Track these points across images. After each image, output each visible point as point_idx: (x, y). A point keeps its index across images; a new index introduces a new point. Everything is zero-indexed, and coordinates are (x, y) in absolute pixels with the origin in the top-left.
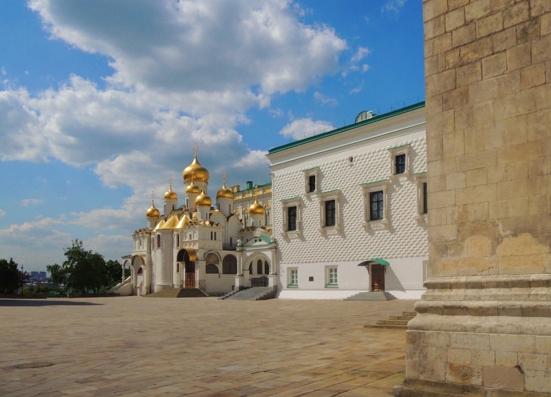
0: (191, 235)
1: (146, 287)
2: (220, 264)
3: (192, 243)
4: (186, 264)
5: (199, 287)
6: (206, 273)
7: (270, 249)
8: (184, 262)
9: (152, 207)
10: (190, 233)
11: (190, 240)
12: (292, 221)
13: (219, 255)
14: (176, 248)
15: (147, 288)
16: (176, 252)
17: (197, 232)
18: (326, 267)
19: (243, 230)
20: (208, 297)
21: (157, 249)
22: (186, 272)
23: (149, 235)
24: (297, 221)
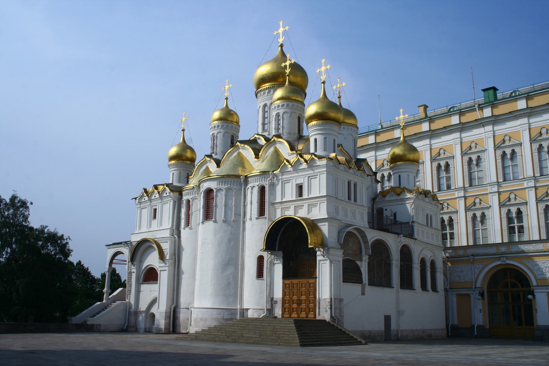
0: (300, 188)
1: (166, 312)
2: (363, 262)
3: (306, 206)
4: (283, 257)
5: (331, 316)
6: (343, 282)
9: (181, 140)
10: (300, 181)
11: (301, 198)
13: (364, 236)
14: (257, 218)
15: (167, 317)
17: (324, 177)
19: (384, 193)
20: (366, 344)
21: (203, 223)
22: (285, 277)
23: (177, 194)
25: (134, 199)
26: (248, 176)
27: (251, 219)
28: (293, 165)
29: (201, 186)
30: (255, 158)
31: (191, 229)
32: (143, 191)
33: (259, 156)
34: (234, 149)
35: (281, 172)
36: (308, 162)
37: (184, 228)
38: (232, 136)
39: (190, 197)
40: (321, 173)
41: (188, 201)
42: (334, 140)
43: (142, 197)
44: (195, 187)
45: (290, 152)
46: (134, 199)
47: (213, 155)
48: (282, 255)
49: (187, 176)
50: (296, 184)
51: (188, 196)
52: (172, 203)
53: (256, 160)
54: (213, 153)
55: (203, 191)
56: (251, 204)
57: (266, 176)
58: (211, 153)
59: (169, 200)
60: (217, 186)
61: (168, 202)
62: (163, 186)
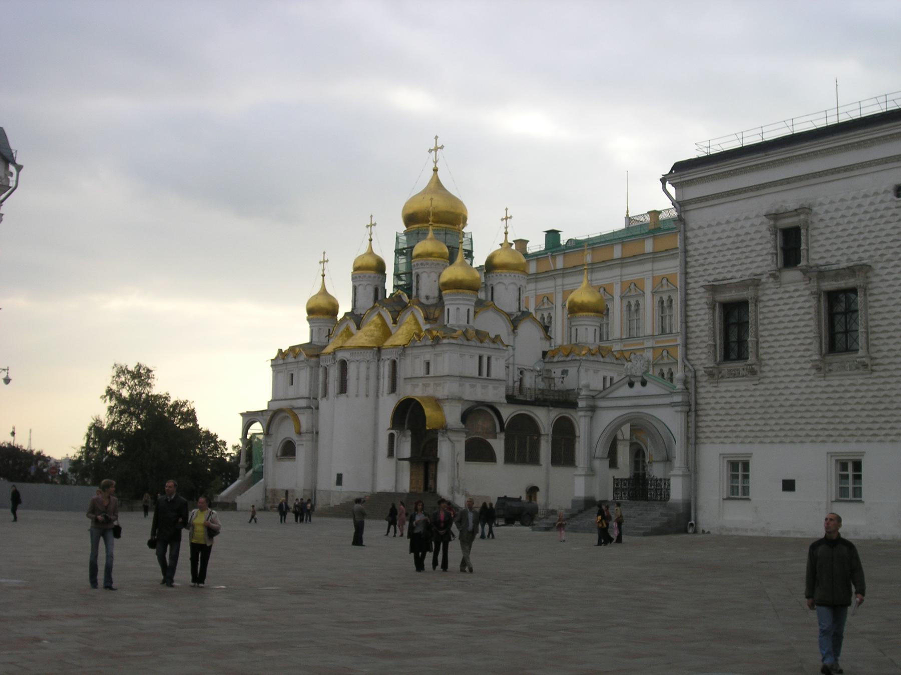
0: (428, 364)
4: (412, 436)
7: (673, 405)
8: (409, 433)
10: (427, 357)
12: (733, 338)
16: (389, 404)
18: (831, 454)
24: (750, 339)
27: (382, 395)
30: (393, 323)
31: (327, 399)
37: (321, 399)
38: (376, 290)
42: (469, 310)
43: (277, 358)
45: (424, 321)
48: (410, 433)
49: (327, 334)
50: (424, 361)
52: (308, 369)
53: (394, 325)
56: (383, 378)
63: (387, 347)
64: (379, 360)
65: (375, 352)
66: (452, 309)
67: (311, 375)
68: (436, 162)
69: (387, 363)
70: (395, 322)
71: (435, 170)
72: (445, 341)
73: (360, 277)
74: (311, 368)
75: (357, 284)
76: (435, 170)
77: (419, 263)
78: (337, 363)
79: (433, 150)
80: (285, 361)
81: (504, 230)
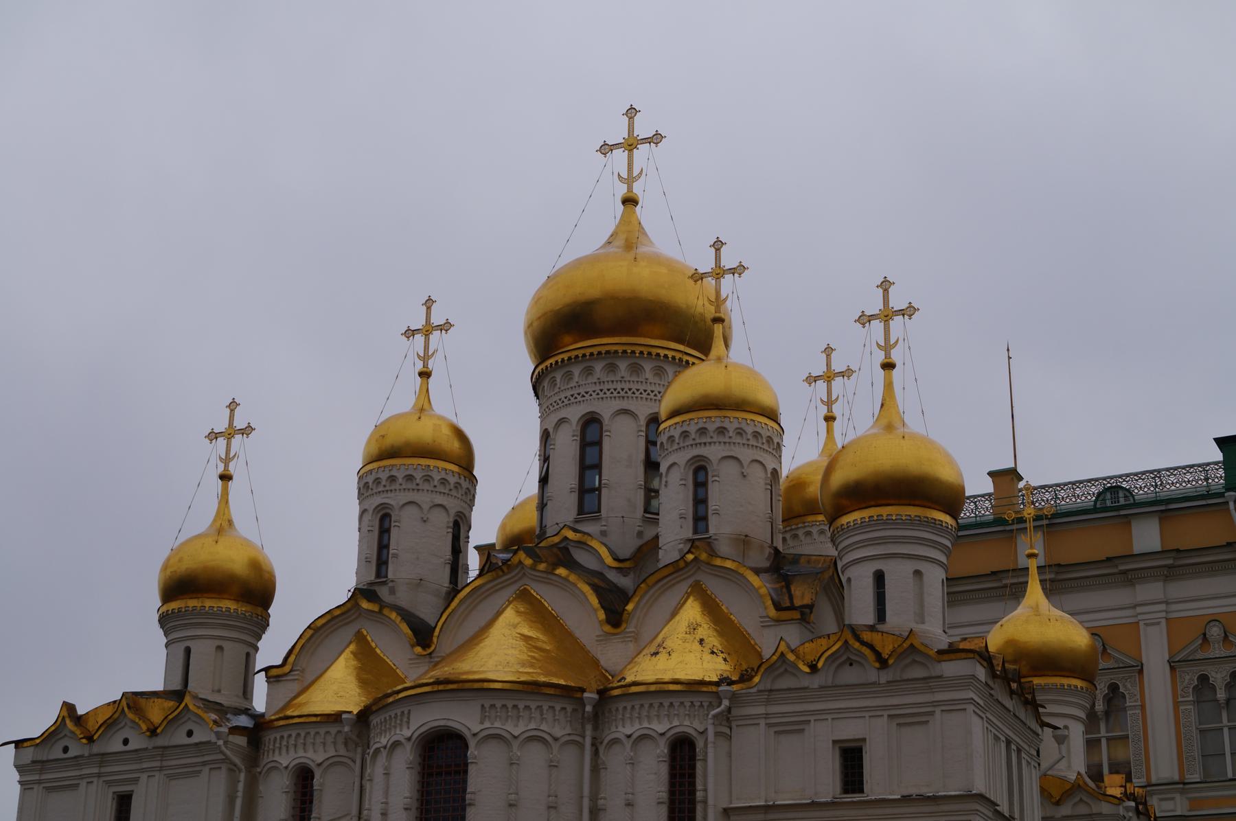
10: (849, 730)
11: (857, 797)
23: (241, 741)
25: (14, 745)
26: (616, 692)
28: (820, 665)
29: (375, 720)
32: (65, 713)
33: (625, 616)
34: (501, 577)
35: (761, 687)
36: (891, 662)
38: (456, 525)
39: (314, 756)
40: (952, 707)
41: (304, 777)
43: (50, 737)
44: (344, 716)
45: (772, 612)
46: (14, 745)
47: (383, 592)
50: (835, 742)
51: (301, 753)
53: (608, 628)
54: (384, 583)
55: (409, 739)
57: (697, 700)
58: (371, 584)
59: (204, 764)
60: (482, 723)
61: (200, 772)
62: (171, 704)
63: (653, 688)
64: (593, 745)
65: (588, 708)
66: (898, 575)
67: (231, 799)
68: (630, 180)
69: (663, 748)
70: (615, 618)
71: (630, 201)
72: (951, 668)
73: (409, 478)
74: (233, 770)
75: (395, 499)
76: (630, 201)
77: (711, 427)
78: (408, 746)
79: (617, 146)
80: (96, 749)
81: (823, 410)
